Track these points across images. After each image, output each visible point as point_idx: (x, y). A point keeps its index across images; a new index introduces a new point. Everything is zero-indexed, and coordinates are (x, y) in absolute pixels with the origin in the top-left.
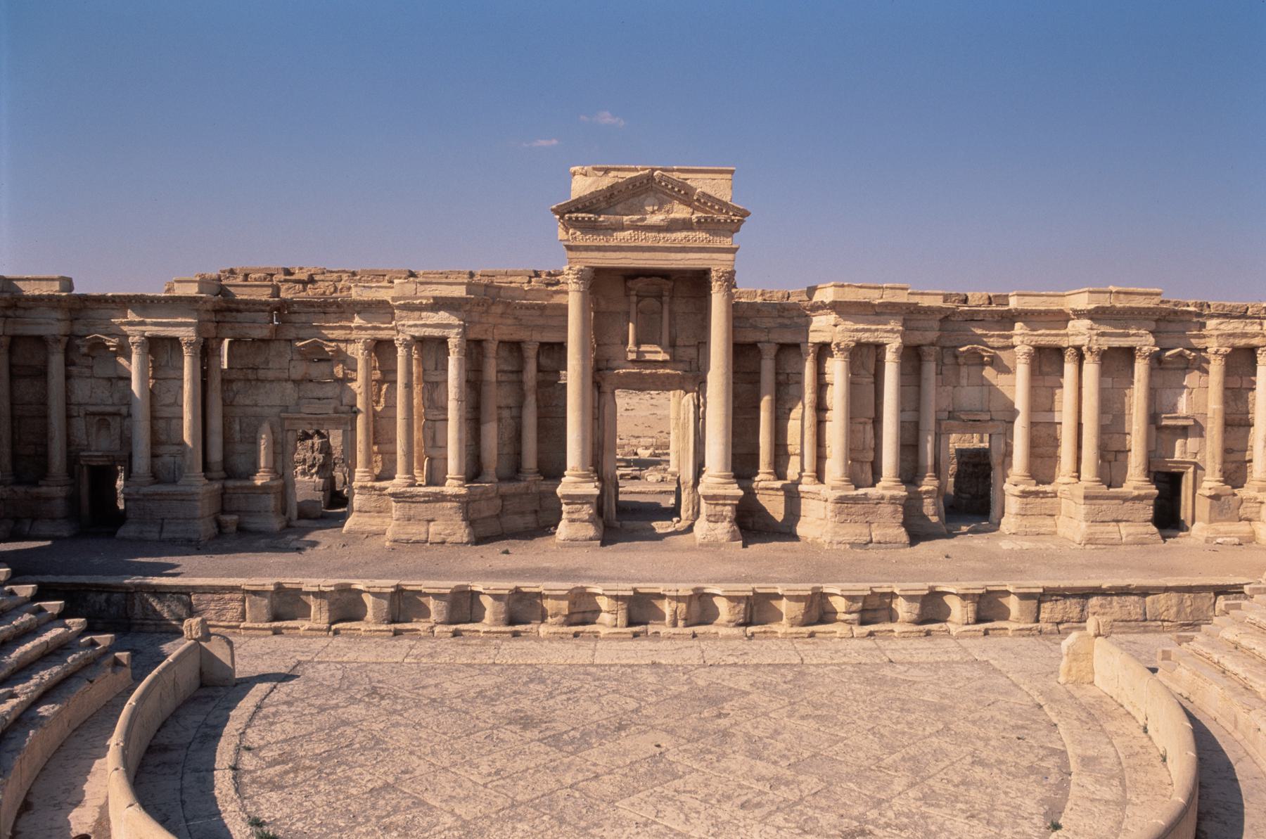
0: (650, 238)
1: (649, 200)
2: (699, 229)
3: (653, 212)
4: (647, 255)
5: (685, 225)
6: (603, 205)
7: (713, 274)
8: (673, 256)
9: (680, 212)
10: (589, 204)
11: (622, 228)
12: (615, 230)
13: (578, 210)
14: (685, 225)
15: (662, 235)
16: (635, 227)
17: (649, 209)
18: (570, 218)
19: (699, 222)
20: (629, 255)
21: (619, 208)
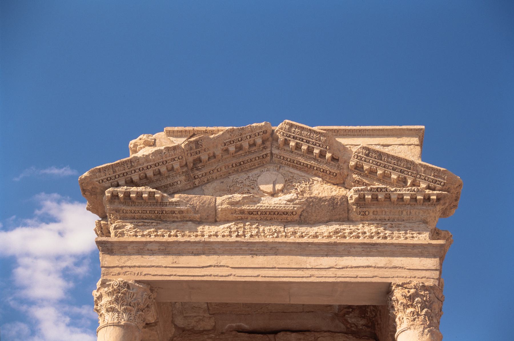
0: (268, 233)
1: (266, 175)
2: (364, 219)
3: (273, 194)
4: (260, 260)
5: (336, 212)
6: (181, 180)
7: (398, 294)
8: (312, 261)
9: (322, 189)
10: (158, 174)
11: (214, 219)
12: (200, 222)
13: (131, 183)
14: (336, 212)
15: (290, 229)
16: (242, 216)
17: (267, 188)
18: (115, 196)
19: (361, 200)
20: (225, 260)
21: (210, 187)
